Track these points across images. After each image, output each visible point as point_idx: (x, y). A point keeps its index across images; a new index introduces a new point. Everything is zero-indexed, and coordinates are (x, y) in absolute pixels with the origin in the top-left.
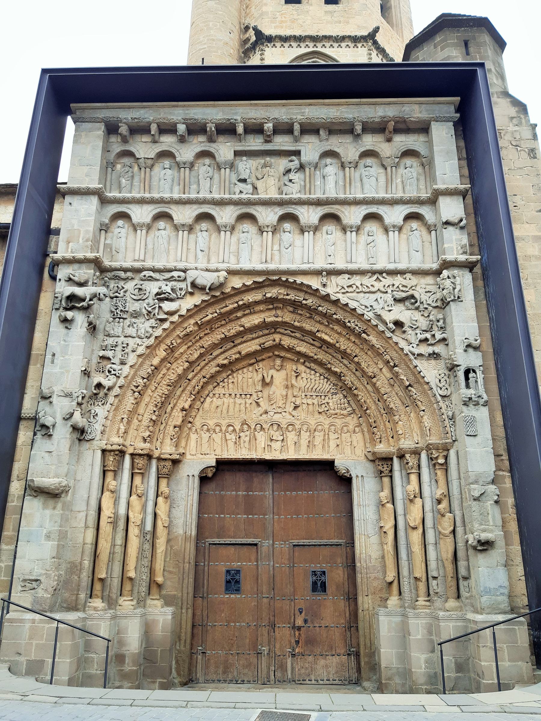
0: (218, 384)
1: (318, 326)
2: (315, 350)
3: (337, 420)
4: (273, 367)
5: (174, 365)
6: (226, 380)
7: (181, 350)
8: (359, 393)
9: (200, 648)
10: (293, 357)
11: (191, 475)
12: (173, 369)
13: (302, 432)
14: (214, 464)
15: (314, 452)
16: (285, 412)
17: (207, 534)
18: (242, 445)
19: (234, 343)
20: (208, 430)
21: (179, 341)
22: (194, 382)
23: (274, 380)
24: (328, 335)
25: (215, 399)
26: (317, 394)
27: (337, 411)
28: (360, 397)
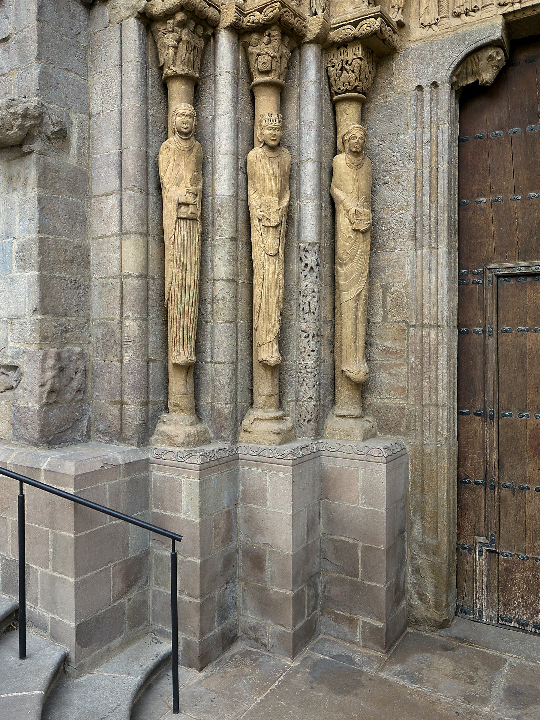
9: (482, 539)
14: (498, 34)
17: (488, 250)
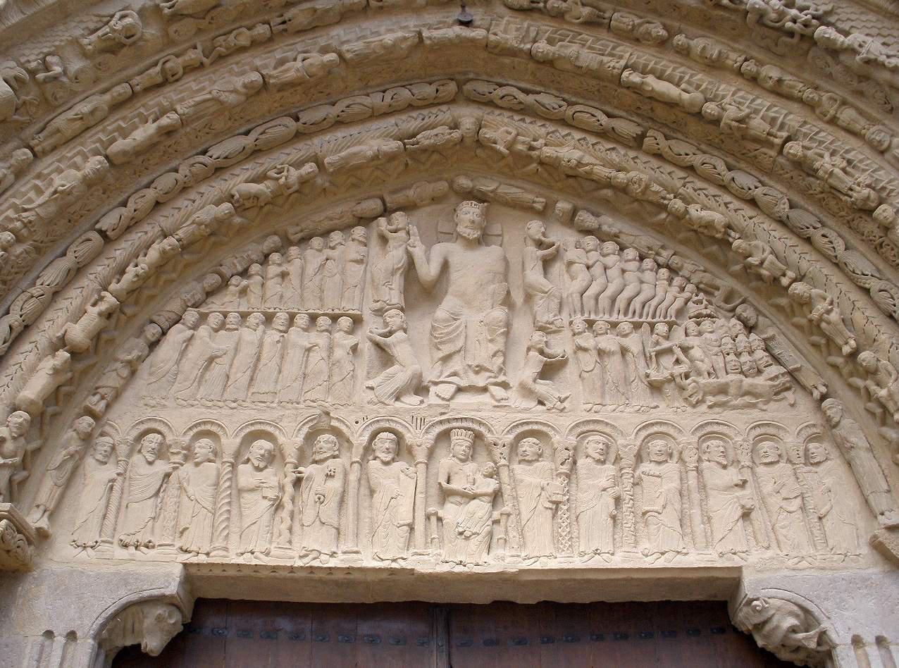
0: (225, 283)
1: (628, 53)
2: (619, 155)
3: (727, 415)
4: (453, 236)
5: (44, 166)
6: (255, 268)
7: (85, 108)
8: (814, 291)
10: (529, 197)
11: (60, 630)
12: (39, 176)
13: (581, 462)
14: (172, 588)
15: (645, 545)
16: (505, 385)
18: (309, 515)
19: (297, 119)
20: (161, 452)
21: (76, 65)
22: (120, 252)
23: (454, 275)
24: (669, 80)
25: (203, 331)
26: (636, 319)
27: (724, 379)
28: (820, 307)
